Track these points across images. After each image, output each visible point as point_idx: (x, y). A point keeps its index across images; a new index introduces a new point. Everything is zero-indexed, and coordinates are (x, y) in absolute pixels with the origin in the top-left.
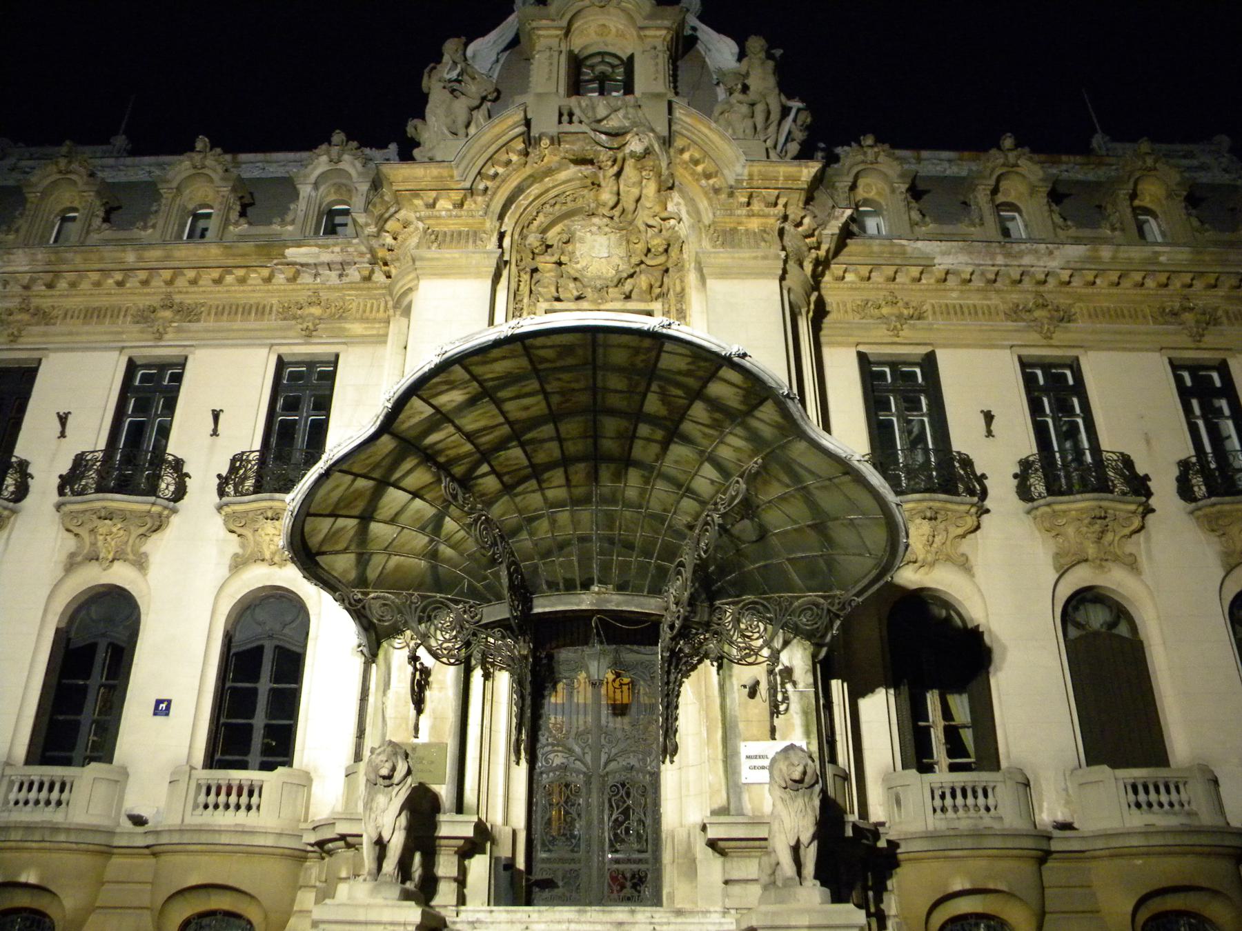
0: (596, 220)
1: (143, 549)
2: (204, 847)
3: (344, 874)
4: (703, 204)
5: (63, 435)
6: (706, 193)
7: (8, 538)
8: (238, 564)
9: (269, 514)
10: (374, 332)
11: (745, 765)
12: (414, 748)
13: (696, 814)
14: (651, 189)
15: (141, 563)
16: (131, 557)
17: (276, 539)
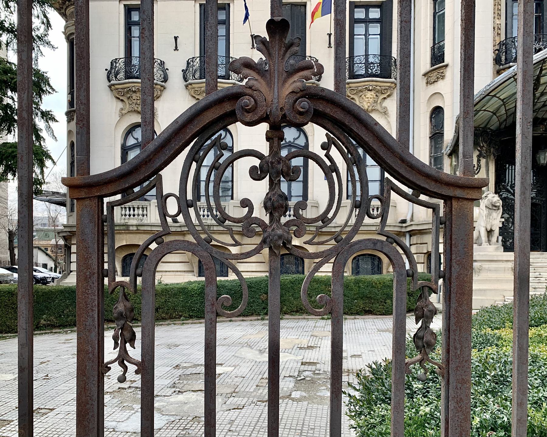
9: (371, 88)
17: (371, 100)
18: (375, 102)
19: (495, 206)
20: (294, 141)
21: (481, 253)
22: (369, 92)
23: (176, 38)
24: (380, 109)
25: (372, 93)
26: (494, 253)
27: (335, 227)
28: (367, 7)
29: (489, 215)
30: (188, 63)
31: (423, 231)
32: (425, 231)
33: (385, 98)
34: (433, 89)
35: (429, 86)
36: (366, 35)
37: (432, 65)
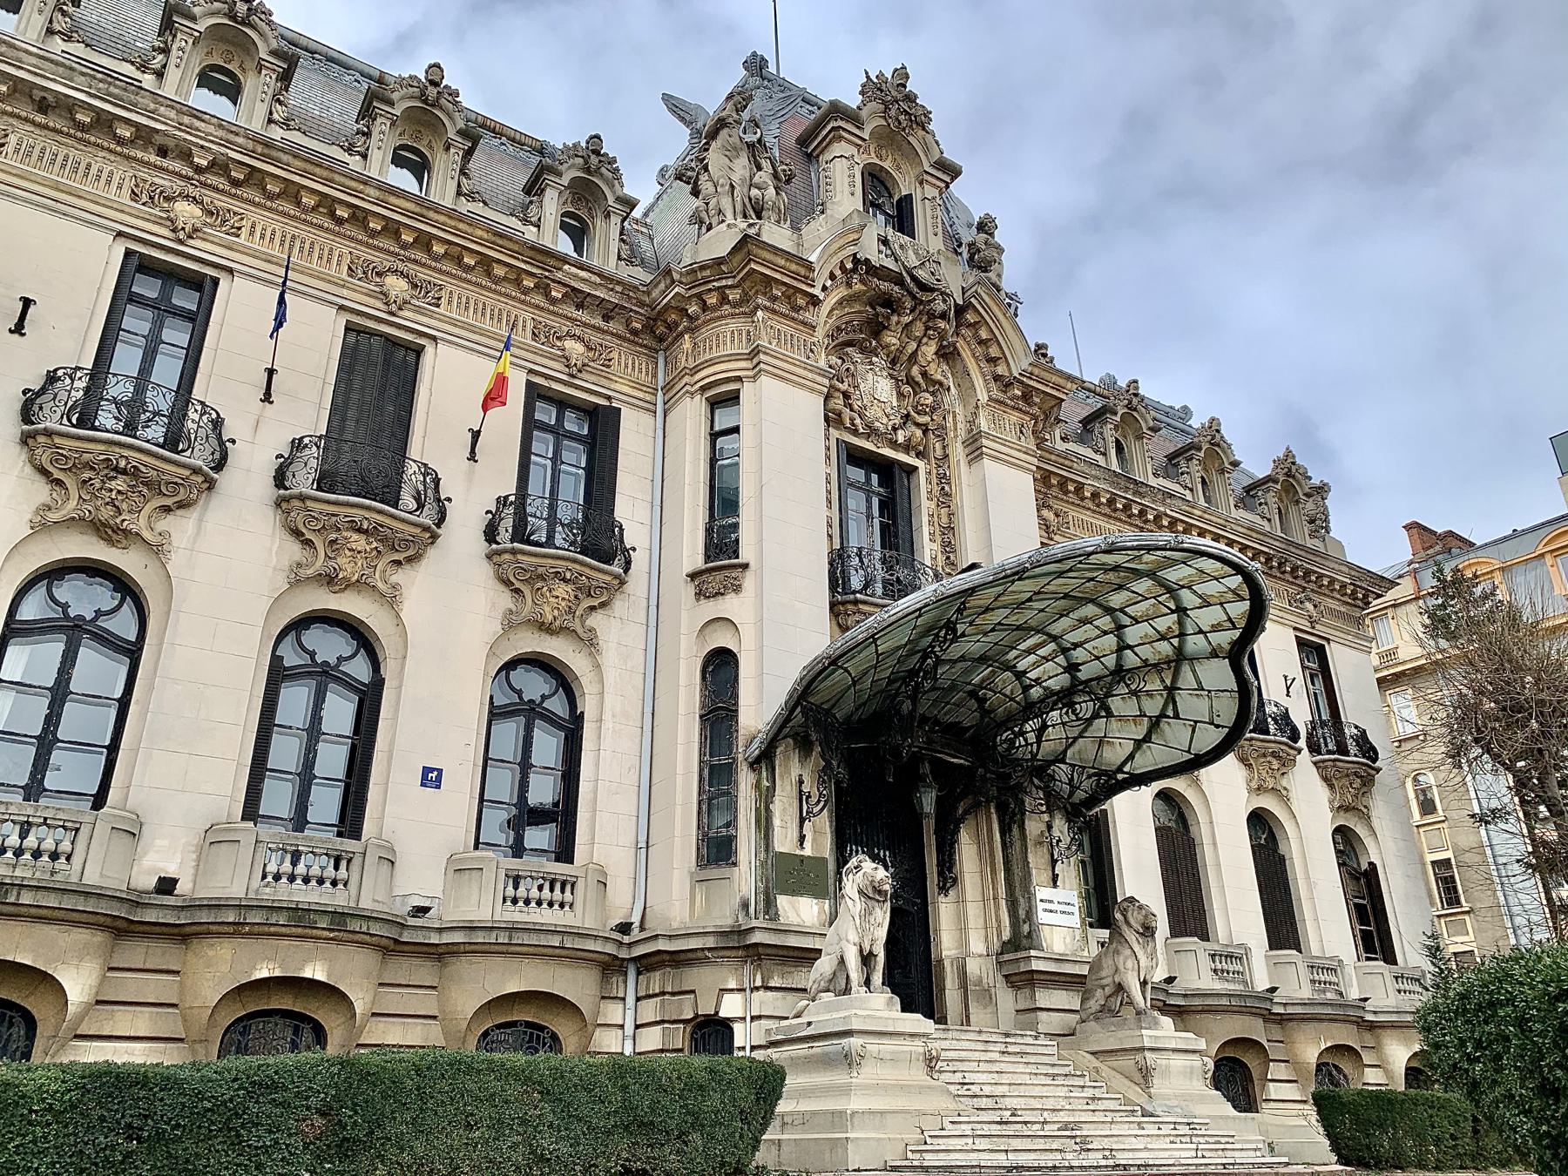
0: (875, 359)
1: (394, 579)
2: (531, 950)
3: (732, 985)
4: (979, 383)
5: (267, 397)
6: (984, 375)
7: (200, 520)
8: (510, 624)
9: (568, 575)
10: (641, 395)
11: (1041, 906)
12: (802, 859)
13: (977, 946)
14: (930, 350)
15: (391, 600)
16: (380, 585)
18: (571, 611)
19: (880, 892)
20: (338, 665)
21: (860, 1012)
22: (563, 585)
23: (27, 303)
24: (580, 631)
25: (569, 588)
26: (886, 1014)
27: (440, 930)
28: (562, 403)
29: (868, 912)
30: (52, 378)
31: (682, 957)
32: (690, 955)
33: (593, 608)
34: (711, 609)
35: (703, 601)
36: (556, 459)
37: (708, 558)
